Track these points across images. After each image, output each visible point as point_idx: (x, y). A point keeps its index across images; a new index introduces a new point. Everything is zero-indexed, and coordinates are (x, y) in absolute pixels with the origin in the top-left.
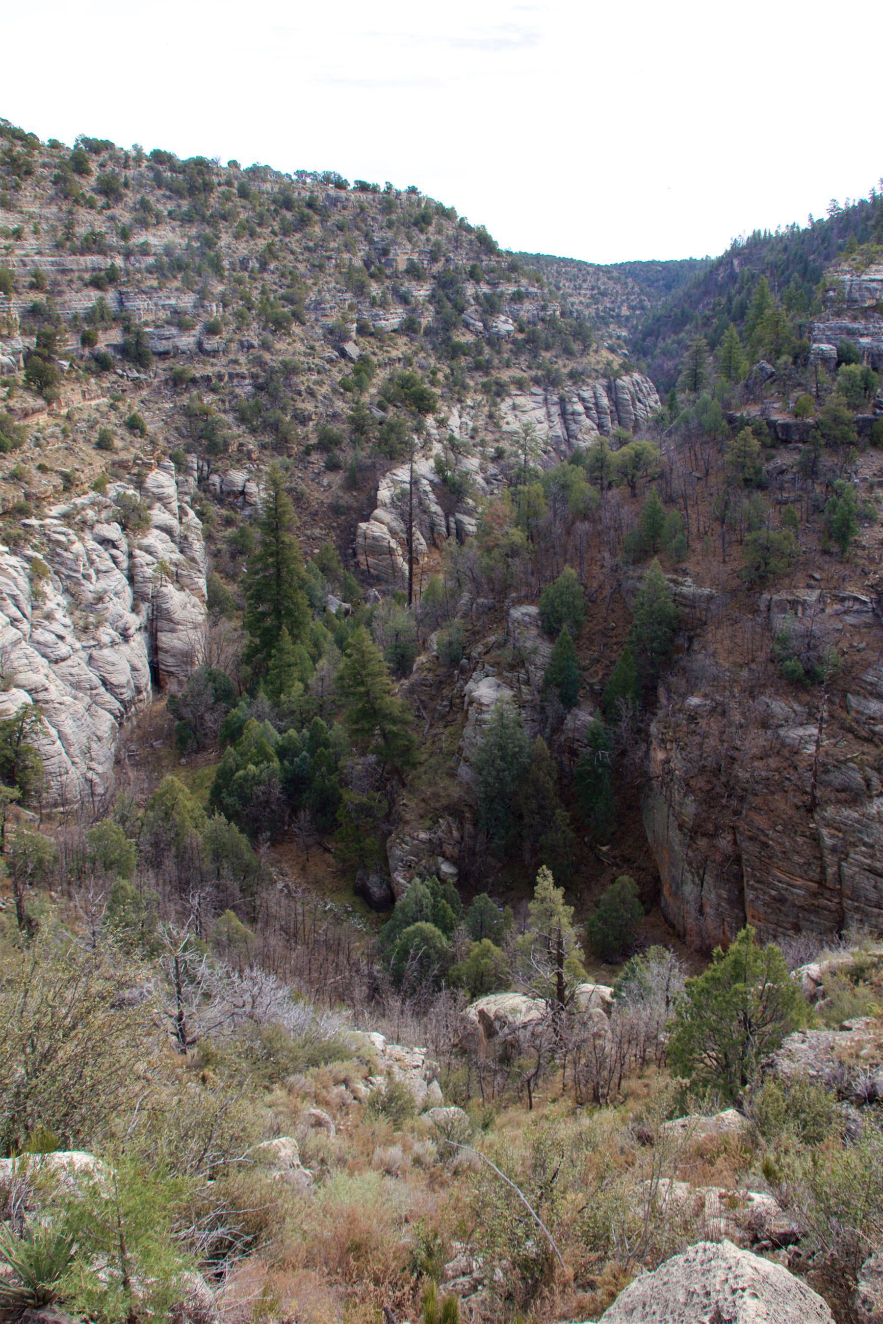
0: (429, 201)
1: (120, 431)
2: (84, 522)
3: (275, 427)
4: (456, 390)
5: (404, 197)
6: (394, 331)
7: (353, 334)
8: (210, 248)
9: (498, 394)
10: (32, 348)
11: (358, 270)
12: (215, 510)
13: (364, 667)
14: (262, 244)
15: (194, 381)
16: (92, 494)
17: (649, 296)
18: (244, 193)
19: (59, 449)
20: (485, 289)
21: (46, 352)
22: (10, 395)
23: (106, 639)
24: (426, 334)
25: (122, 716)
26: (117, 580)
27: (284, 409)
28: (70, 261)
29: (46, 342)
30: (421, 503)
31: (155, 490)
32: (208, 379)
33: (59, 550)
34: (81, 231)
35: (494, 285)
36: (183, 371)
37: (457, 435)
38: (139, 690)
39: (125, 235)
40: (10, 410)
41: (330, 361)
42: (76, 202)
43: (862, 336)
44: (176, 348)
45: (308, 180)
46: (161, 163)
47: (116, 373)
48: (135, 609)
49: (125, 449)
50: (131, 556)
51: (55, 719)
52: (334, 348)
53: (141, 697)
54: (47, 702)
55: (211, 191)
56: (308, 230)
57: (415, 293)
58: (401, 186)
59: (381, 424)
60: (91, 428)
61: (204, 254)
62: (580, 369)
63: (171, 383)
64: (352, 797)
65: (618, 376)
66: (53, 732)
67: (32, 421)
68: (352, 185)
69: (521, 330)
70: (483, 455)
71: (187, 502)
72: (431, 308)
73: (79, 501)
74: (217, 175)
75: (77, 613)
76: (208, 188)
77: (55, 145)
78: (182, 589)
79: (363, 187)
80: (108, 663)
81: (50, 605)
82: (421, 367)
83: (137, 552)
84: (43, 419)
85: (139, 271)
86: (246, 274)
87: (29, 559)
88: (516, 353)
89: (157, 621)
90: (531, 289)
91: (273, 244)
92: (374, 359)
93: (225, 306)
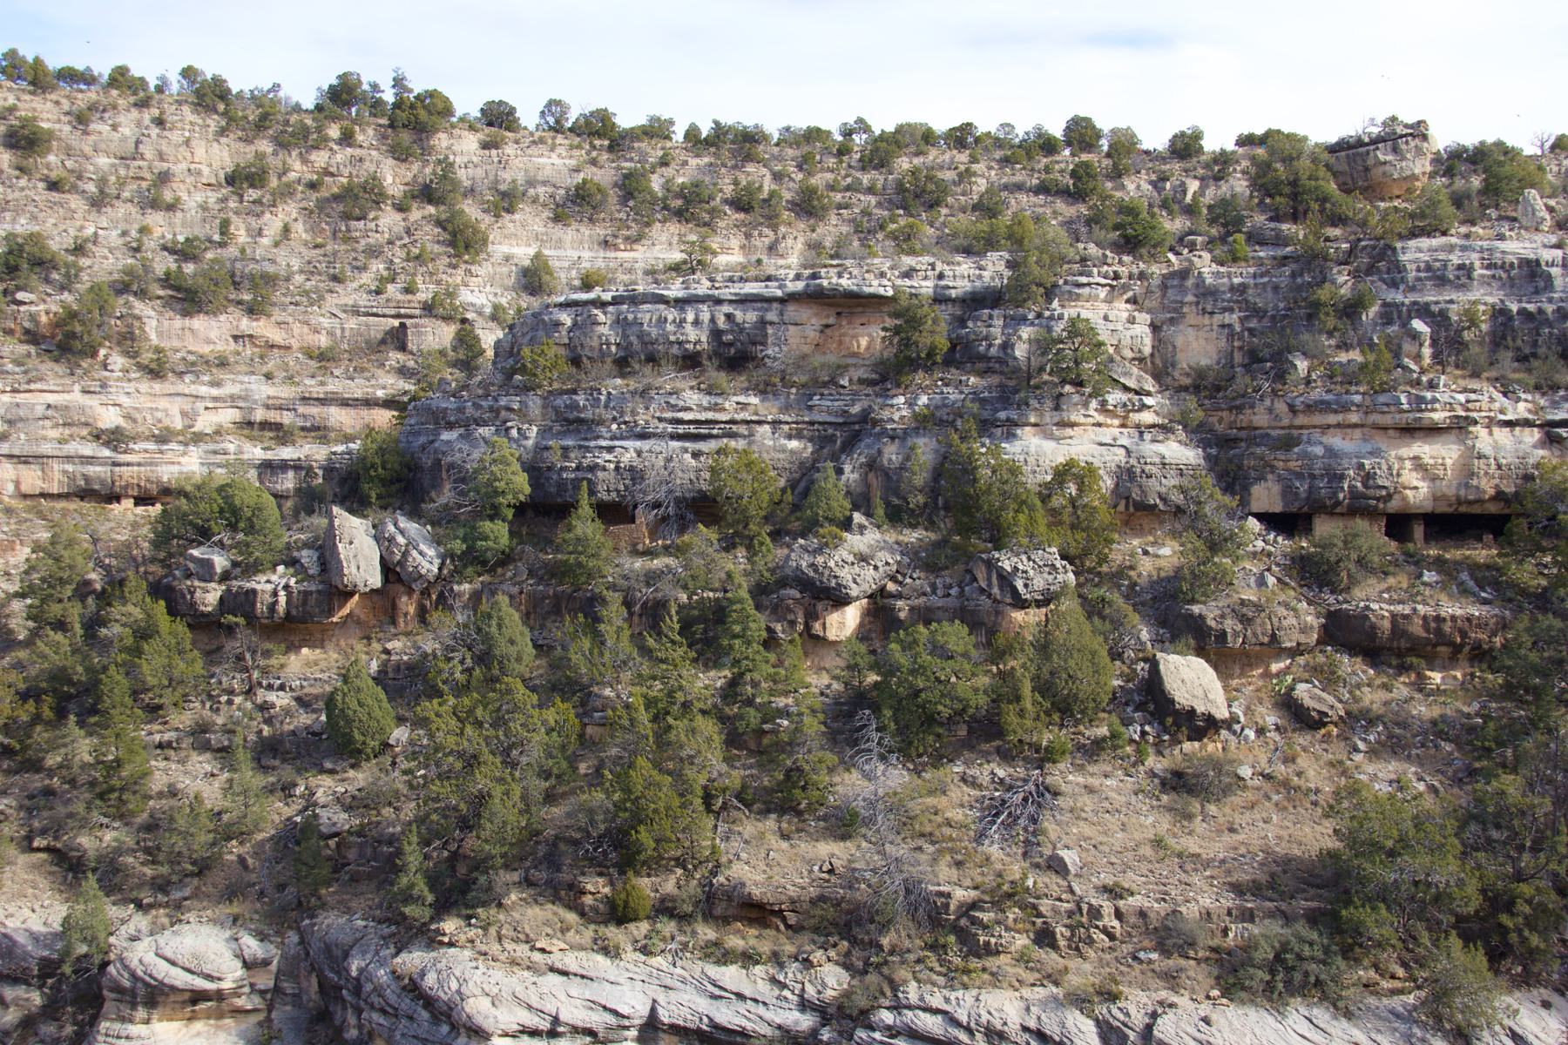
43: (450, 426)
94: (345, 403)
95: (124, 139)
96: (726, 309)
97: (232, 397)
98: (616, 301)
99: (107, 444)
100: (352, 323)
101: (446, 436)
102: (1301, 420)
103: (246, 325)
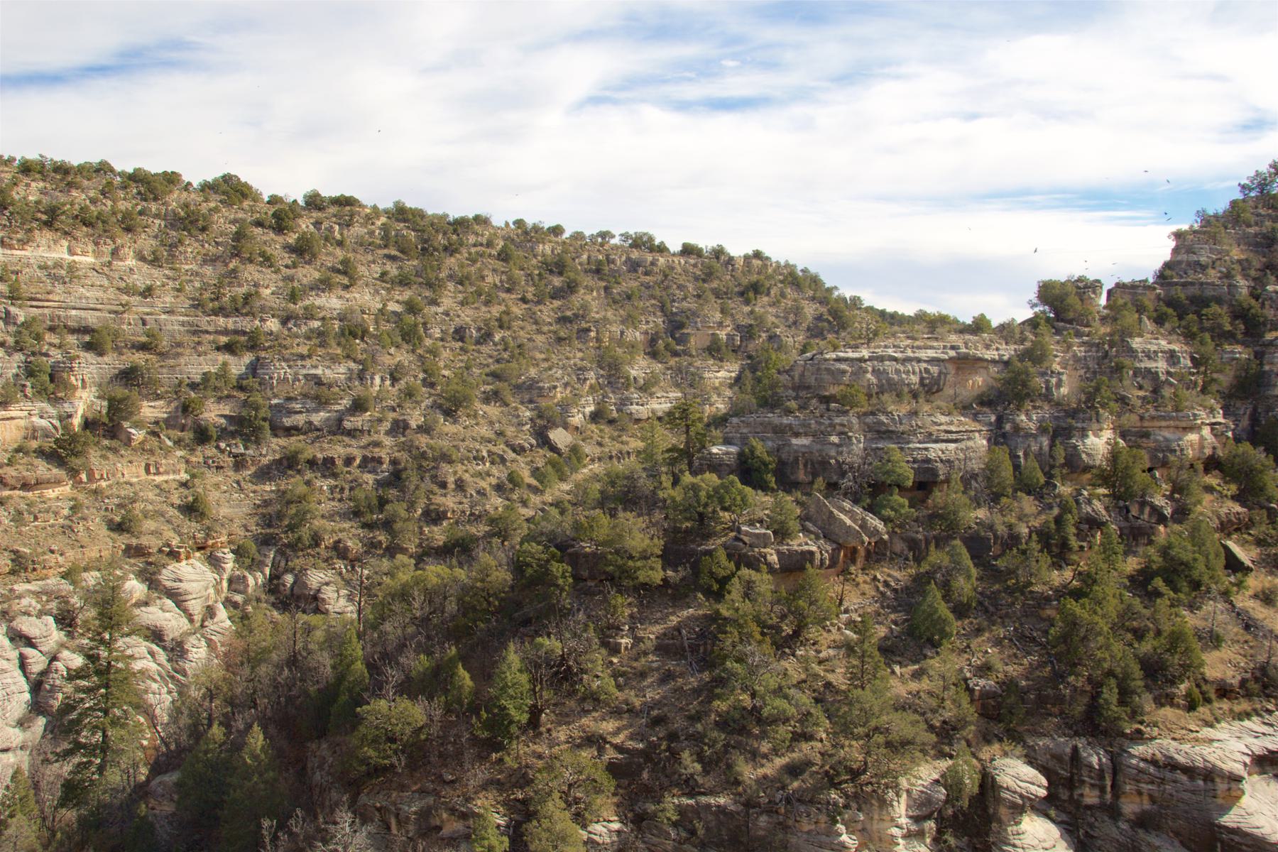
1: (172, 512)
14: (496, 310)
15: (312, 463)
28: (204, 321)
31: (169, 584)
32: (329, 462)
39: (293, 297)
41: (519, 450)
43: (797, 435)
44: (310, 423)
47: (218, 447)
48: (22, 723)
57: (706, 375)
60: (120, 506)
63: (285, 463)
72: (728, 393)
76: (450, 250)
79: (688, 250)
93: (394, 380)
96: (924, 365)
98: (870, 359)
101: (794, 441)
102: (1146, 424)
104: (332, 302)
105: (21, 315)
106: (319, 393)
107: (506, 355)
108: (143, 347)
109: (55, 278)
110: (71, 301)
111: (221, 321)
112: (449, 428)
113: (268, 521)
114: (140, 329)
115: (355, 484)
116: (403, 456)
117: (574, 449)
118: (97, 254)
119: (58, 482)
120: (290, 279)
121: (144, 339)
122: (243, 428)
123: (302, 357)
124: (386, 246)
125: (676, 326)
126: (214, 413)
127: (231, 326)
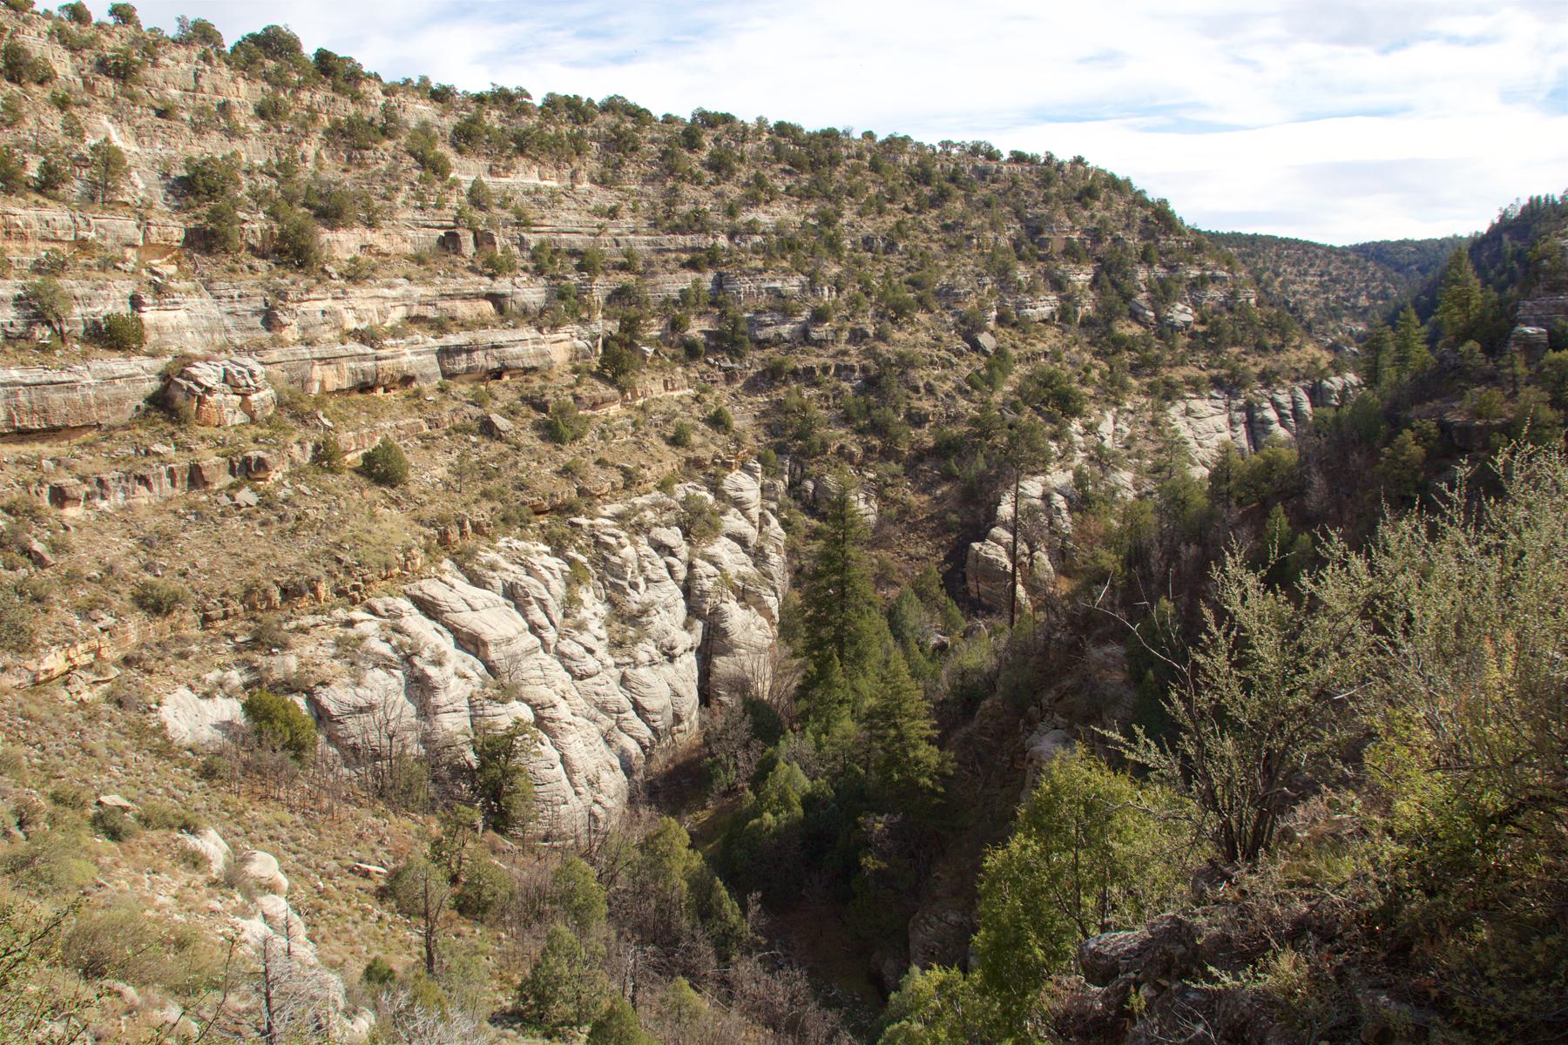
0: (1098, 172)
1: (702, 426)
2: (640, 525)
3: (879, 429)
4: (1112, 392)
5: (1068, 167)
6: (1044, 321)
7: (991, 325)
8: (829, 225)
9: (1167, 397)
10: (615, 333)
11: (1005, 251)
12: (804, 521)
13: (899, 706)
14: (890, 221)
15: (794, 373)
16: (656, 494)
17: (1395, 283)
18: (875, 167)
19: (626, 443)
20: (1161, 272)
21: (627, 338)
22: (578, 383)
23: (643, 657)
24: (1082, 324)
25: (653, 746)
26: (671, 592)
27: (896, 409)
28: (665, 239)
29: (630, 326)
30: (1051, 523)
31: (732, 493)
33: (605, 553)
34: (685, 208)
35: (1172, 268)
36: (782, 363)
37: (1108, 443)
38: (678, 719)
39: (731, 212)
40: (576, 398)
42: (683, 178)
44: (779, 335)
45: (955, 151)
46: (784, 135)
47: (707, 362)
48: (687, 626)
49: (703, 445)
50: (691, 566)
51: (560, 740)
52: (965, 339)
53: (681, 727)
54: (553, 720)
55: (838, 164)
56: (948, 205)
57: (1073, 278)
58: (1064, 155)
59: (1011, 427)
60: (667, 421)
61: (822, 233)
62: (1275, 367)
63: (768, 375)
64: (870, 862)
65: (1323, 375)
66: (556, 755)
67: (601, 412)
68: (1006, 156)
69: (1203, 322)
70: (1138, 469)
71: (772, 511)
72: (1092, 295)
73: (639, 501)
74: (847, 147)
75: (616, 625)
76: (834, 161)
77: (668, 119)
78: (746, 607)
79: (1018, 158)
80: (642, 684)
81: (585, 614)
82: (1073, 363)
83: (698, 562)
84: (614, 409)
85: (744, 251)
86: (870, 255)
87: (571, 562)
88: (1192, 348)
89: (713, 642)
90: (1219, 273)
91: (903, 222)
92: (1014, 353)
93: (839, 291)
94: (464, 298)
95: (185, 73)
97: (404, 297)
99: (363, 341)
100: (422, 233)
103: (371, 237)
104: (763, 217)
105: (533, 240)
106: (782, 306)
107: (913, 263)
108: (623, 267)
109: (541, 203)
110: (559, 225)
111: (680, 239)
112: (897, 335)
113: (772, 430)
114: (614, 250)
115: (839, 393)
116: (869, 363)
117: (998, 351)
118: (560, 178)
119: (612, 401)
120: (719, 195)
121: (621, 259)
122: (727, 341)
123: (760, 271)
124: (779, 161)
125: (1034, 230)
126: (697, 328)
127: (689, 244)
